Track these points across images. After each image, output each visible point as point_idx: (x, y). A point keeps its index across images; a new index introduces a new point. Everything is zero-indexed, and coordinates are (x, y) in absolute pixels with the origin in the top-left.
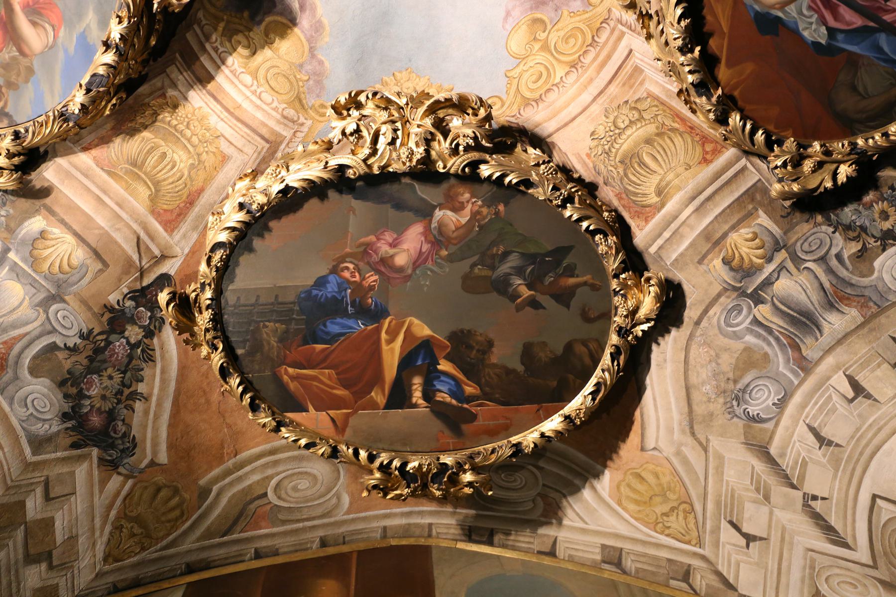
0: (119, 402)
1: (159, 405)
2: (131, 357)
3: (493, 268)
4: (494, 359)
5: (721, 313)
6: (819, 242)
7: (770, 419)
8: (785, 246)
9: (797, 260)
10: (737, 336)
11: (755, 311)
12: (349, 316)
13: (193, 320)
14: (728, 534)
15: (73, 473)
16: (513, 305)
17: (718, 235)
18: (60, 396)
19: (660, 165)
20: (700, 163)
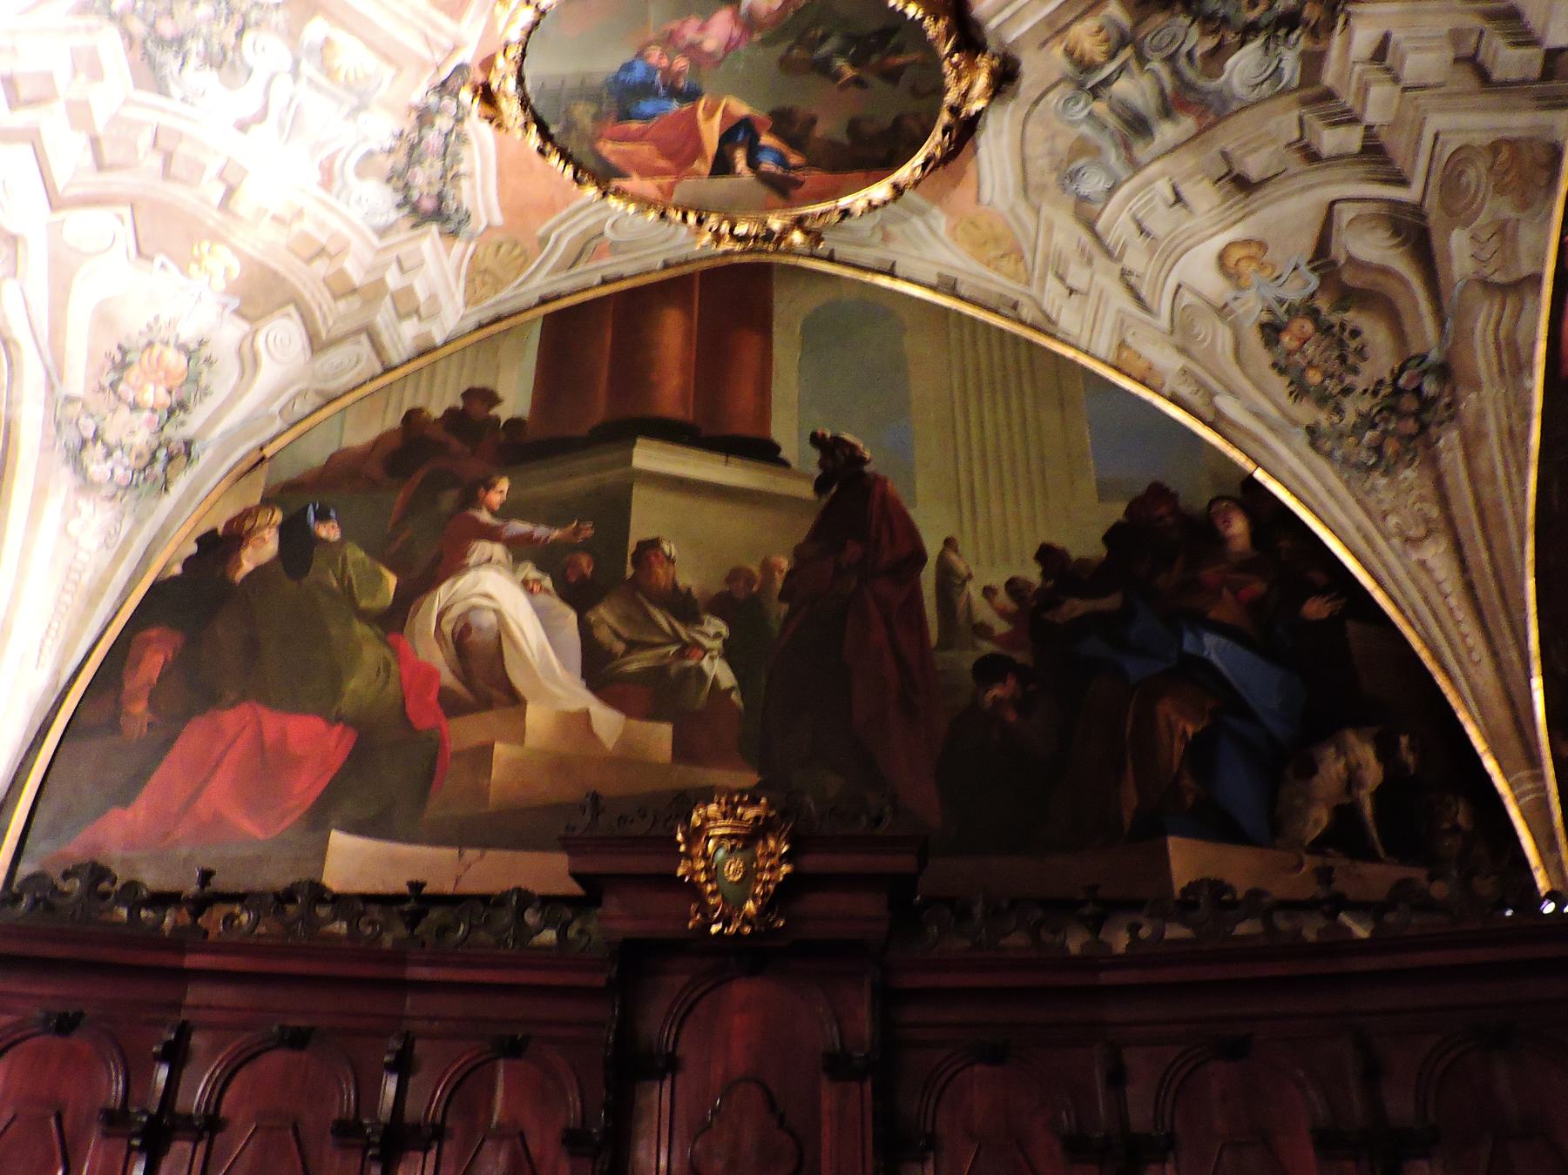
5: (1059, 100)
9: (1142, 59)
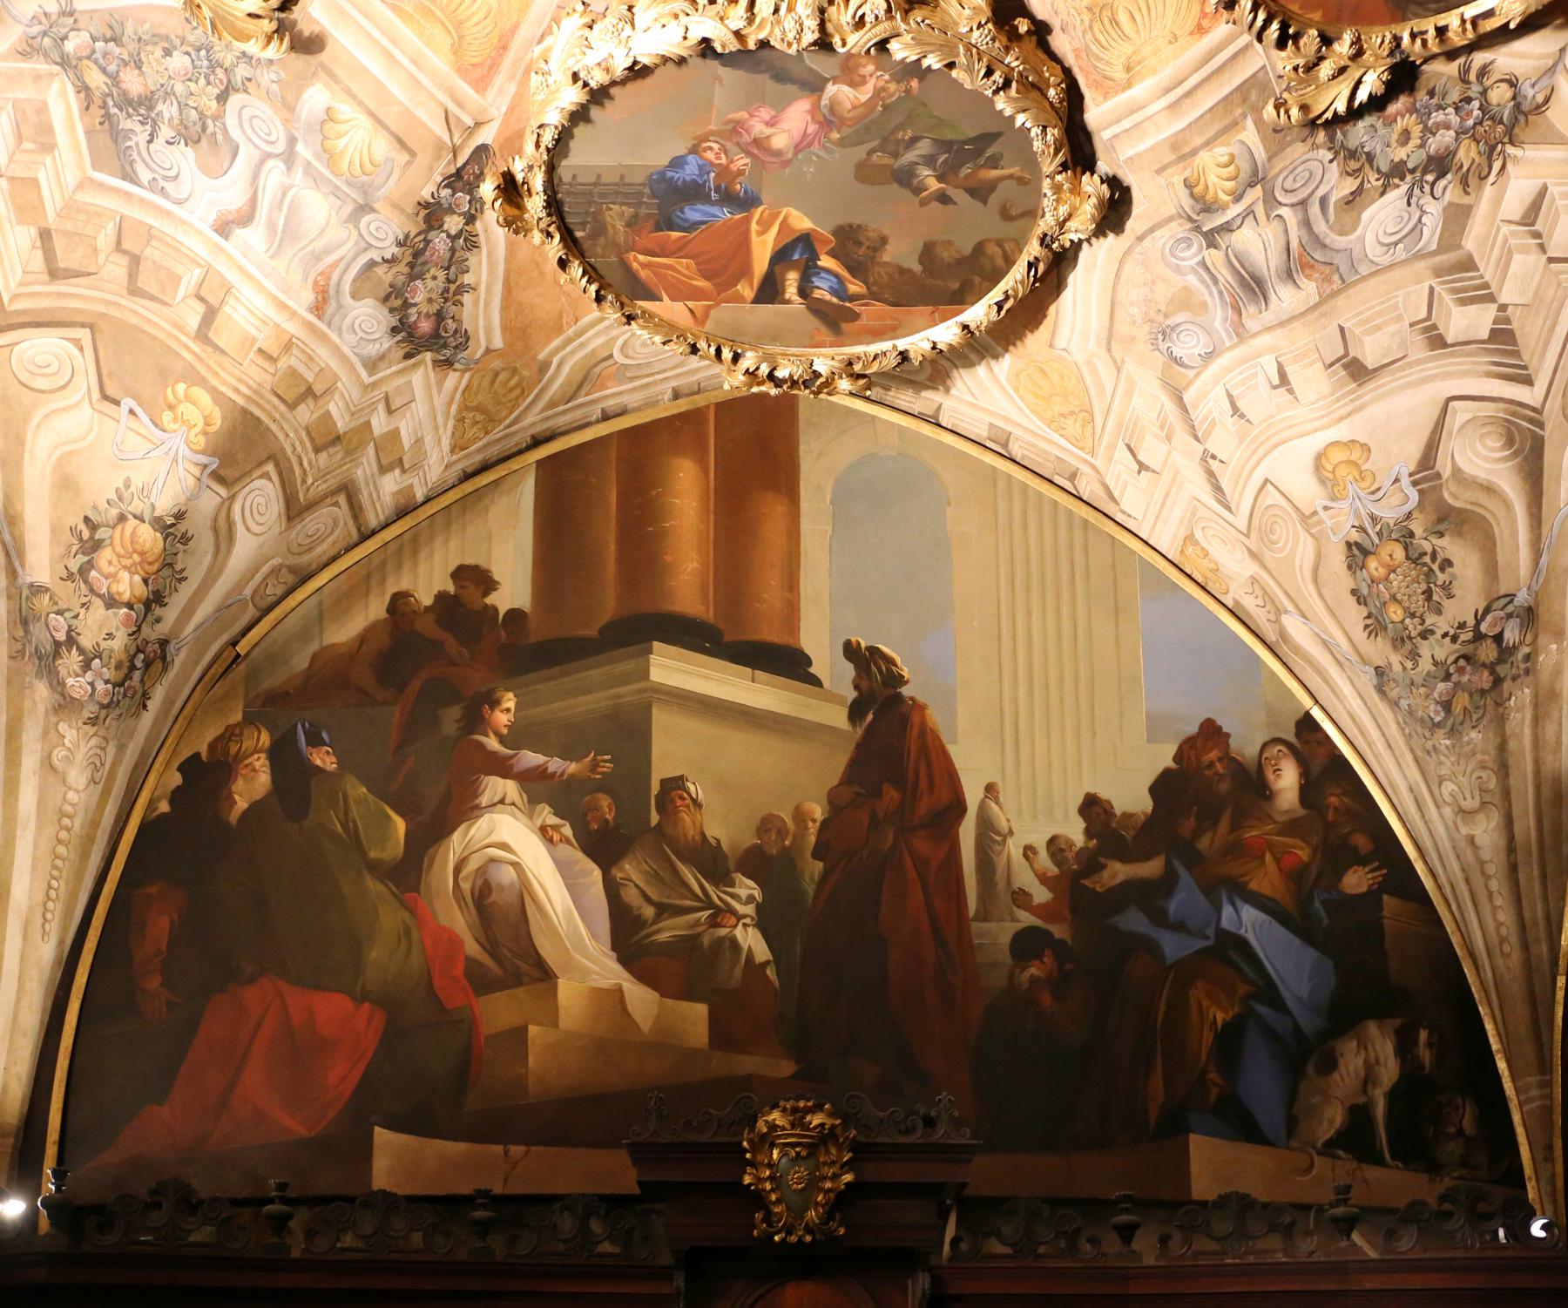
0: (446, 300)
1: (489, 290)
2: (453, 250)
3: (896, 155)
4: (886, 257)
6: (1307, 174)
7: (1192, 367)
8: (1263, 179)
9: (1270, 201)
10: (1177, 269)
11: (1206, 253)
12: (713, 203)
13: (521, 207)
14: (1121, 453)
15: (410, 382)
16: (917, 200)
17: (1186, 150)
18: (386, 312)
19: (1138, 31)
20: (1191, 33)
